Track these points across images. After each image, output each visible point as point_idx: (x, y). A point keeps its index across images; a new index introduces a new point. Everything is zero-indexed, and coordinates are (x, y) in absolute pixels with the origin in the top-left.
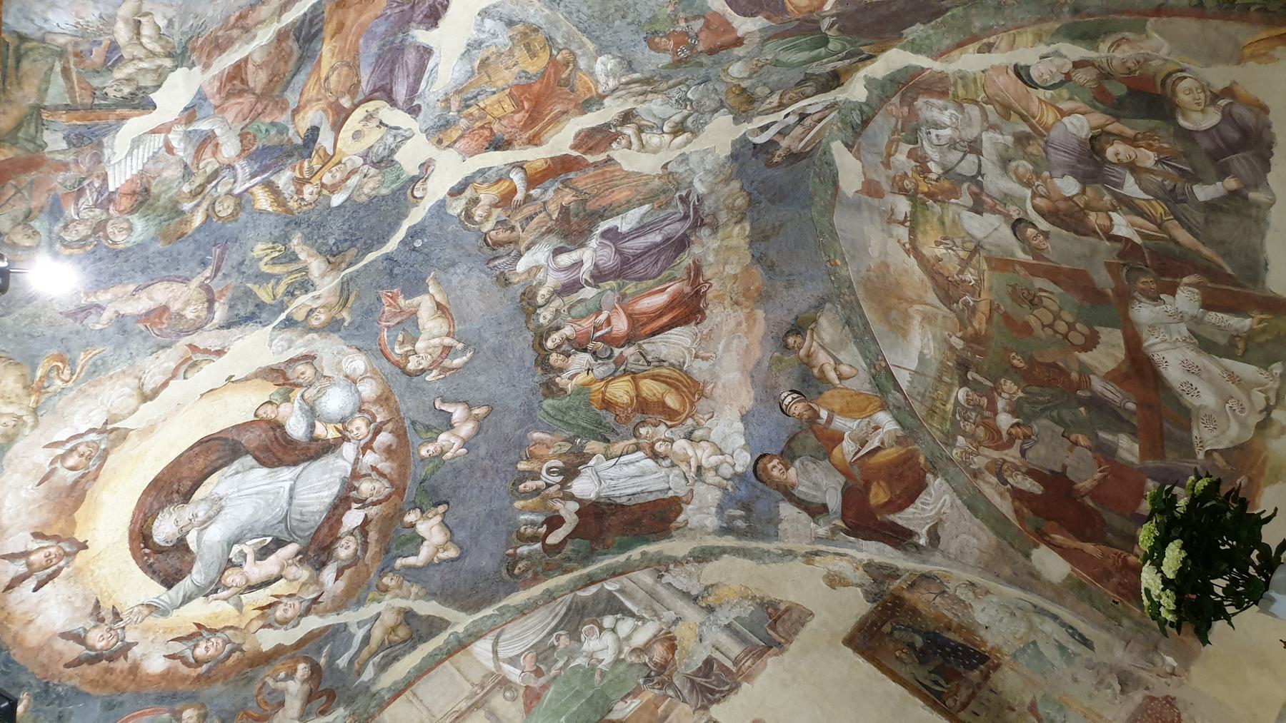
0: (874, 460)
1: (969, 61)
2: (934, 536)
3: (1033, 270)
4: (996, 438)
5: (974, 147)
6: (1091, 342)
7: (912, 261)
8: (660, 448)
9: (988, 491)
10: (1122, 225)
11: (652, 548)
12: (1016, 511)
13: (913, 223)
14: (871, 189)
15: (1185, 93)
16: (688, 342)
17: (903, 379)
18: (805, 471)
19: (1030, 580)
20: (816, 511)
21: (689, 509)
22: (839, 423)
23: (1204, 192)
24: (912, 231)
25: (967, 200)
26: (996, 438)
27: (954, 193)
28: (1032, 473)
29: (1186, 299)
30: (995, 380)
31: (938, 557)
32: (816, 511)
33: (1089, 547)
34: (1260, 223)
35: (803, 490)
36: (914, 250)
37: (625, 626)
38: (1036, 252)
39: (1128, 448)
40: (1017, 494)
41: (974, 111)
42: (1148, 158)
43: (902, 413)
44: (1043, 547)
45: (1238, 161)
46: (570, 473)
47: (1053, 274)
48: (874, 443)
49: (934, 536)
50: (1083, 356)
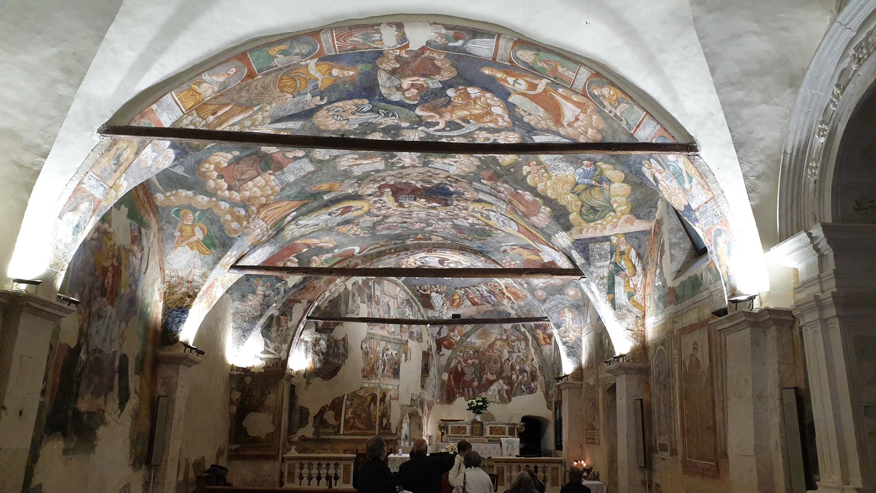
0: (452, 340)
1: (533, 351)
2: (442, 355)
3: (501, 362)
4: (465, 361)
5: (519, 351)
6: (492, 374)
7: (494, 339)
8: (445, 305)
9: (454, 360)
10: (514, 377)
11: (420, 306)
12: (453, 368)
13: (501, 339)
14: (506, 331)
15: (535, 383)
16: (468, 304)
17: (469, 339)
18: (446, 329)
19: (440, 374)
20: (439, 333)
21: (432, 311)
22: (456, 331)
23: (523, 387)
24: (500, 339)
25: (510, 350)
26: (465, 361)
27: (510, 348)
28: (462, 368)
29: (506, 387)
30: (477, 358)
31: (438, 357)
32: (439, 333)
33: (453, 382)
34: (521, 395)
35: (443, 330)
36: (496, 340)
37: (411, 313)
38: (505, 363)
39: (476, 384)
40: (456, 367)
41: (525, 351)
42: (525, 379)
43: (461, 341)
44: (448, 374)
45: (528, 391)
46: (437, 292)
47: (502, 366)
48: (454, 338)
49: (442, 355)
50: (489, 373)
